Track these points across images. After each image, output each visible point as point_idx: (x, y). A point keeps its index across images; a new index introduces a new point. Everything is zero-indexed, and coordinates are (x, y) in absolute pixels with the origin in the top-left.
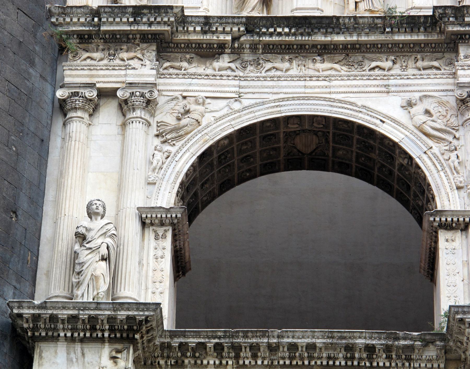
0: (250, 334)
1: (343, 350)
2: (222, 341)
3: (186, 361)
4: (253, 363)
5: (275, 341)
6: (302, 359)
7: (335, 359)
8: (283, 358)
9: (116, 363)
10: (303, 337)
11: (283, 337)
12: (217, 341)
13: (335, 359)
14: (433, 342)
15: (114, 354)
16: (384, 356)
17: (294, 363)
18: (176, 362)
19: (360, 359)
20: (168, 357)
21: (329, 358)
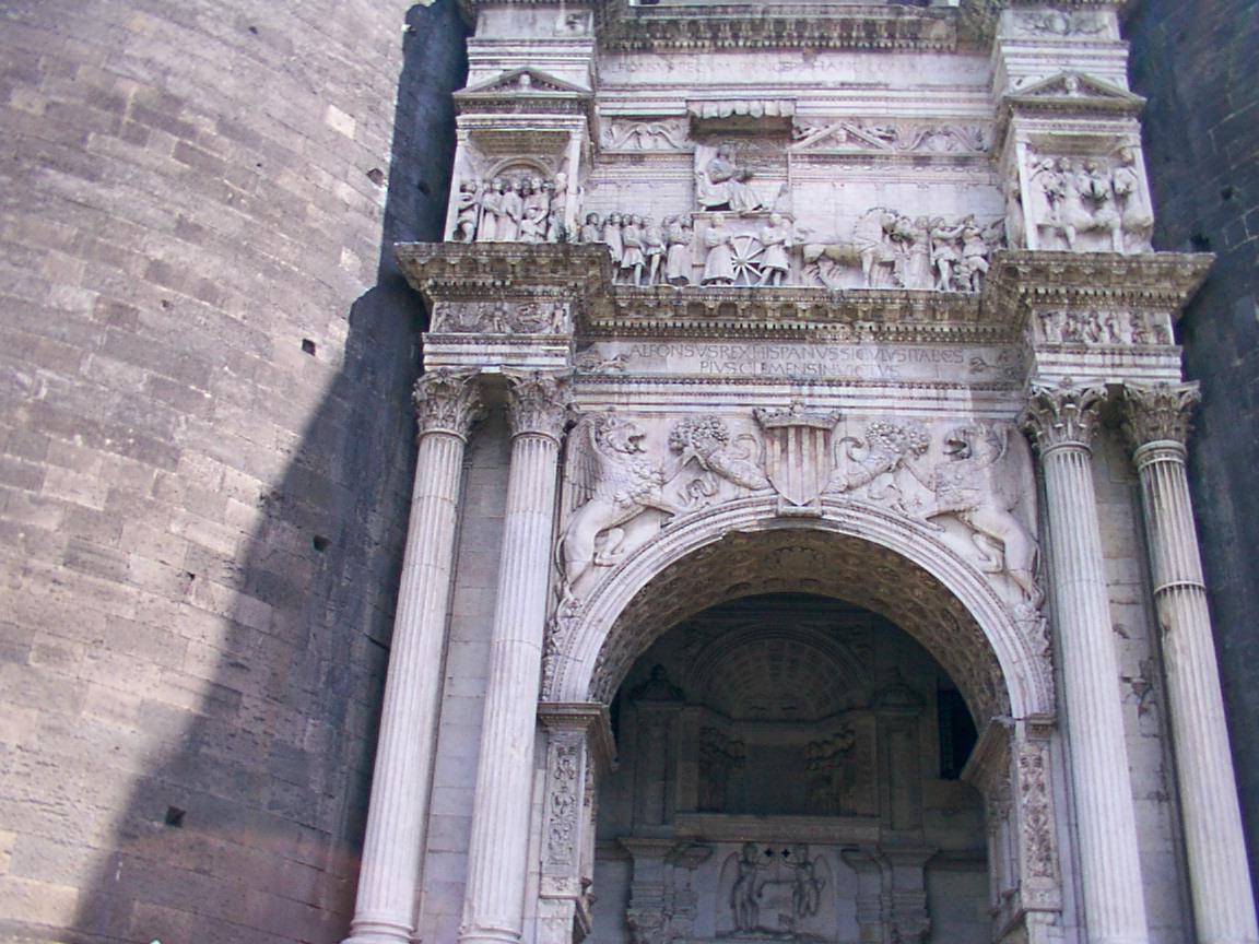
0: (730, 10)
1: (838, 28)
2: (698, 17)
3: (656, 43)
4: (733, 44)
5: (759, 16)
6: (790, 37)
7: (829, 38)
8: (769, 38)
9: (573, 28)
10: (792, 13)
11: (768, 12)
12: (691, 18)
13: (829, 38)
14: (943, 18)
15: (571, 19)
16: (886, 35)
17: (781, 44)
18: (644, 45)
19: (858, 39)
20: (635, 39)
21: (822, 37)
